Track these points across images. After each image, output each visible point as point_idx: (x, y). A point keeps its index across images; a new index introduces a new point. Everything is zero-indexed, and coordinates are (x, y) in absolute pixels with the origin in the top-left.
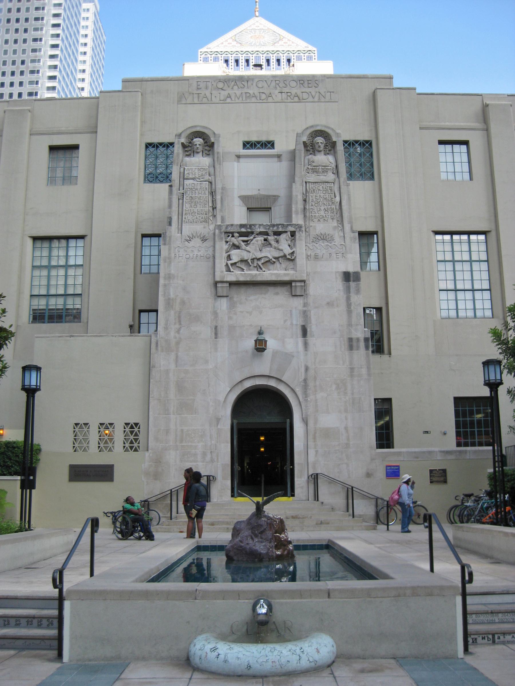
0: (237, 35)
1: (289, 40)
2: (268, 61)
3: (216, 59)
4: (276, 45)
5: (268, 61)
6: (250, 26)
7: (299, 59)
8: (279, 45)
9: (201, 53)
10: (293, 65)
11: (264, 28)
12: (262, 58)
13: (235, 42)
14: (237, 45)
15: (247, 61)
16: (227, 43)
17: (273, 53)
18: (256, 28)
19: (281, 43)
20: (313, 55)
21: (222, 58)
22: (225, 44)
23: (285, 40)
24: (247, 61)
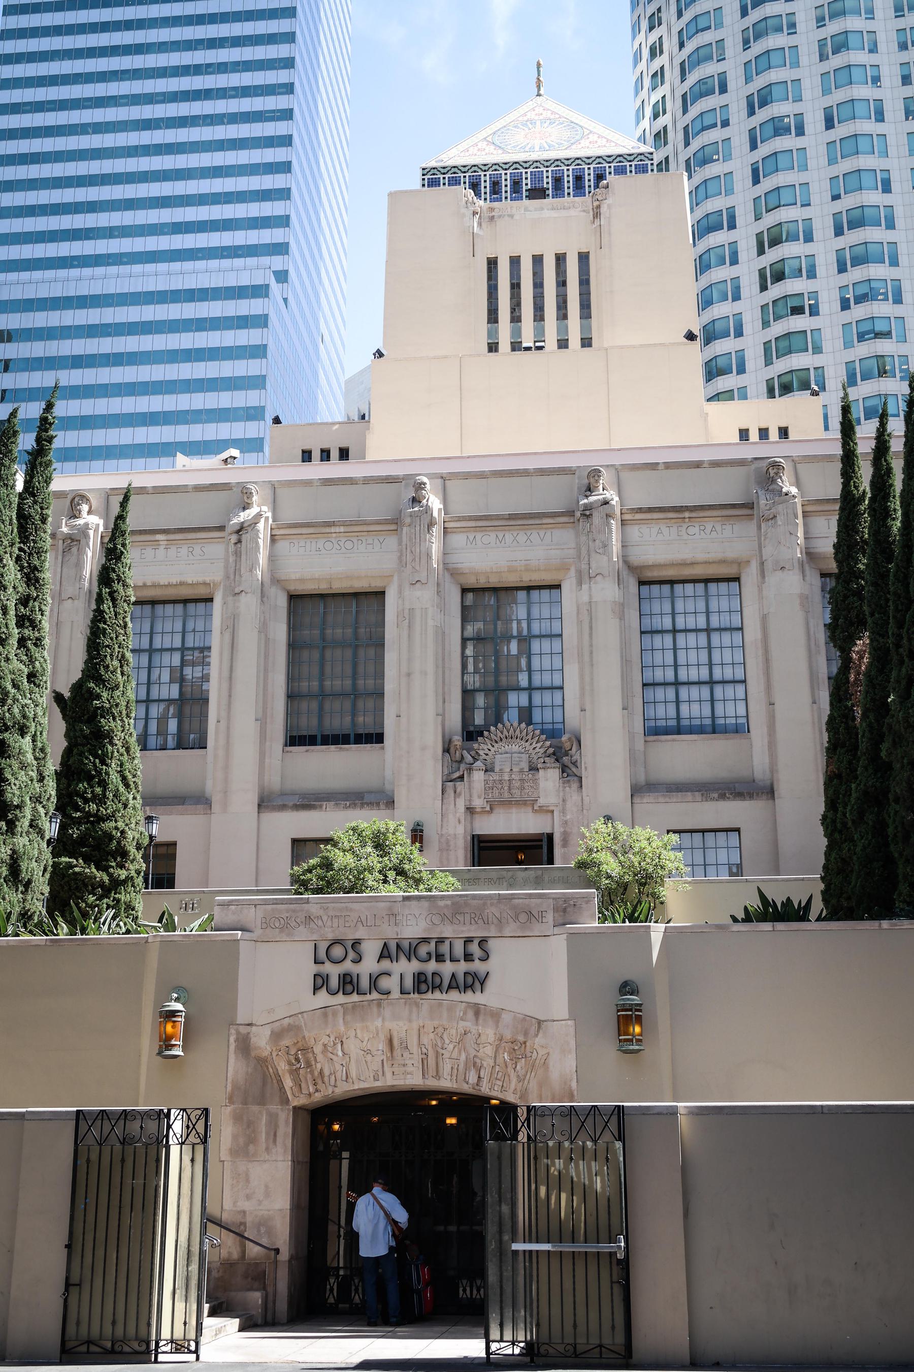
1: (600, 136)
2: (558, 181)
3: (454, 182)
4: (574, 147)
5: (558, 181)
7: (620, 171)
8: (580, 146)
9: (425, 172)
10: (607, 187)
11: (552, 117)
12: (545, 175)
13: (493, 147)
14: (495, 152)
15: (516, 185)
16: (476, 148)
17: (568, 162)
18: (537, 118)
20: (649, 162)
23: (593, 138)
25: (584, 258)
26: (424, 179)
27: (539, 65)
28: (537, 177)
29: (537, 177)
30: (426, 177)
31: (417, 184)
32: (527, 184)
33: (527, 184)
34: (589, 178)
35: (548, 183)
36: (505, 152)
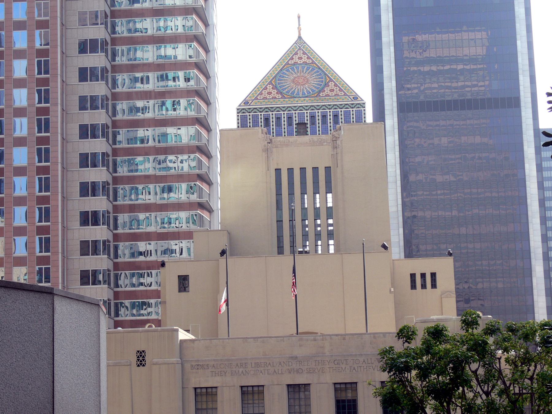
0: (278, 77)
2: (313, 117)
3: (255, 124)
4: (321, 95)
5: (313, 117)
6: (292, 59)
9: (239, 110)
15: (290, 118)
19: (327, 90)
20: (363, 109)
21: (261, 116)
22: (265, 92)
23: (331, 84)
24: (290, 118)
25: (328, 169)
26: (238, 116)
27: (299, 17)
28: (301, 116)
29: (301, 116)
30: (239, 114)
31: (234, 125)
32: (296, 121)
33: (296, 121)
34: (330, 119)
35: (307, 120)
36: (283, 97)
